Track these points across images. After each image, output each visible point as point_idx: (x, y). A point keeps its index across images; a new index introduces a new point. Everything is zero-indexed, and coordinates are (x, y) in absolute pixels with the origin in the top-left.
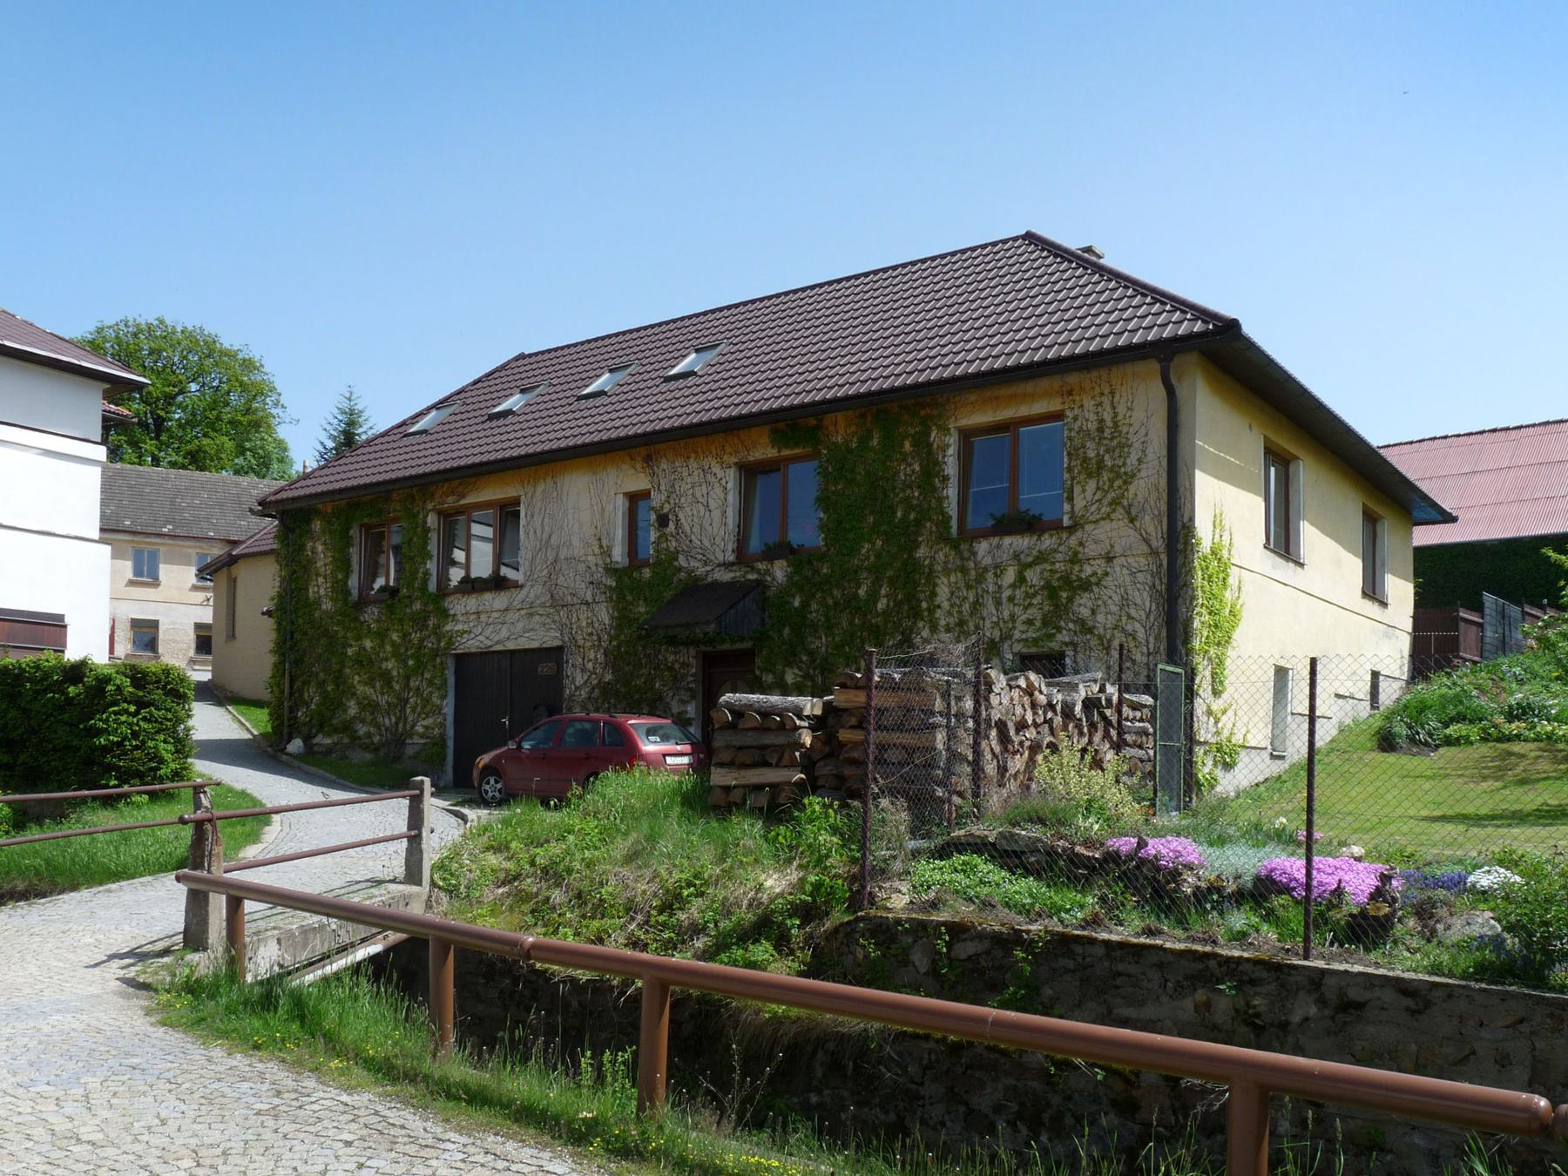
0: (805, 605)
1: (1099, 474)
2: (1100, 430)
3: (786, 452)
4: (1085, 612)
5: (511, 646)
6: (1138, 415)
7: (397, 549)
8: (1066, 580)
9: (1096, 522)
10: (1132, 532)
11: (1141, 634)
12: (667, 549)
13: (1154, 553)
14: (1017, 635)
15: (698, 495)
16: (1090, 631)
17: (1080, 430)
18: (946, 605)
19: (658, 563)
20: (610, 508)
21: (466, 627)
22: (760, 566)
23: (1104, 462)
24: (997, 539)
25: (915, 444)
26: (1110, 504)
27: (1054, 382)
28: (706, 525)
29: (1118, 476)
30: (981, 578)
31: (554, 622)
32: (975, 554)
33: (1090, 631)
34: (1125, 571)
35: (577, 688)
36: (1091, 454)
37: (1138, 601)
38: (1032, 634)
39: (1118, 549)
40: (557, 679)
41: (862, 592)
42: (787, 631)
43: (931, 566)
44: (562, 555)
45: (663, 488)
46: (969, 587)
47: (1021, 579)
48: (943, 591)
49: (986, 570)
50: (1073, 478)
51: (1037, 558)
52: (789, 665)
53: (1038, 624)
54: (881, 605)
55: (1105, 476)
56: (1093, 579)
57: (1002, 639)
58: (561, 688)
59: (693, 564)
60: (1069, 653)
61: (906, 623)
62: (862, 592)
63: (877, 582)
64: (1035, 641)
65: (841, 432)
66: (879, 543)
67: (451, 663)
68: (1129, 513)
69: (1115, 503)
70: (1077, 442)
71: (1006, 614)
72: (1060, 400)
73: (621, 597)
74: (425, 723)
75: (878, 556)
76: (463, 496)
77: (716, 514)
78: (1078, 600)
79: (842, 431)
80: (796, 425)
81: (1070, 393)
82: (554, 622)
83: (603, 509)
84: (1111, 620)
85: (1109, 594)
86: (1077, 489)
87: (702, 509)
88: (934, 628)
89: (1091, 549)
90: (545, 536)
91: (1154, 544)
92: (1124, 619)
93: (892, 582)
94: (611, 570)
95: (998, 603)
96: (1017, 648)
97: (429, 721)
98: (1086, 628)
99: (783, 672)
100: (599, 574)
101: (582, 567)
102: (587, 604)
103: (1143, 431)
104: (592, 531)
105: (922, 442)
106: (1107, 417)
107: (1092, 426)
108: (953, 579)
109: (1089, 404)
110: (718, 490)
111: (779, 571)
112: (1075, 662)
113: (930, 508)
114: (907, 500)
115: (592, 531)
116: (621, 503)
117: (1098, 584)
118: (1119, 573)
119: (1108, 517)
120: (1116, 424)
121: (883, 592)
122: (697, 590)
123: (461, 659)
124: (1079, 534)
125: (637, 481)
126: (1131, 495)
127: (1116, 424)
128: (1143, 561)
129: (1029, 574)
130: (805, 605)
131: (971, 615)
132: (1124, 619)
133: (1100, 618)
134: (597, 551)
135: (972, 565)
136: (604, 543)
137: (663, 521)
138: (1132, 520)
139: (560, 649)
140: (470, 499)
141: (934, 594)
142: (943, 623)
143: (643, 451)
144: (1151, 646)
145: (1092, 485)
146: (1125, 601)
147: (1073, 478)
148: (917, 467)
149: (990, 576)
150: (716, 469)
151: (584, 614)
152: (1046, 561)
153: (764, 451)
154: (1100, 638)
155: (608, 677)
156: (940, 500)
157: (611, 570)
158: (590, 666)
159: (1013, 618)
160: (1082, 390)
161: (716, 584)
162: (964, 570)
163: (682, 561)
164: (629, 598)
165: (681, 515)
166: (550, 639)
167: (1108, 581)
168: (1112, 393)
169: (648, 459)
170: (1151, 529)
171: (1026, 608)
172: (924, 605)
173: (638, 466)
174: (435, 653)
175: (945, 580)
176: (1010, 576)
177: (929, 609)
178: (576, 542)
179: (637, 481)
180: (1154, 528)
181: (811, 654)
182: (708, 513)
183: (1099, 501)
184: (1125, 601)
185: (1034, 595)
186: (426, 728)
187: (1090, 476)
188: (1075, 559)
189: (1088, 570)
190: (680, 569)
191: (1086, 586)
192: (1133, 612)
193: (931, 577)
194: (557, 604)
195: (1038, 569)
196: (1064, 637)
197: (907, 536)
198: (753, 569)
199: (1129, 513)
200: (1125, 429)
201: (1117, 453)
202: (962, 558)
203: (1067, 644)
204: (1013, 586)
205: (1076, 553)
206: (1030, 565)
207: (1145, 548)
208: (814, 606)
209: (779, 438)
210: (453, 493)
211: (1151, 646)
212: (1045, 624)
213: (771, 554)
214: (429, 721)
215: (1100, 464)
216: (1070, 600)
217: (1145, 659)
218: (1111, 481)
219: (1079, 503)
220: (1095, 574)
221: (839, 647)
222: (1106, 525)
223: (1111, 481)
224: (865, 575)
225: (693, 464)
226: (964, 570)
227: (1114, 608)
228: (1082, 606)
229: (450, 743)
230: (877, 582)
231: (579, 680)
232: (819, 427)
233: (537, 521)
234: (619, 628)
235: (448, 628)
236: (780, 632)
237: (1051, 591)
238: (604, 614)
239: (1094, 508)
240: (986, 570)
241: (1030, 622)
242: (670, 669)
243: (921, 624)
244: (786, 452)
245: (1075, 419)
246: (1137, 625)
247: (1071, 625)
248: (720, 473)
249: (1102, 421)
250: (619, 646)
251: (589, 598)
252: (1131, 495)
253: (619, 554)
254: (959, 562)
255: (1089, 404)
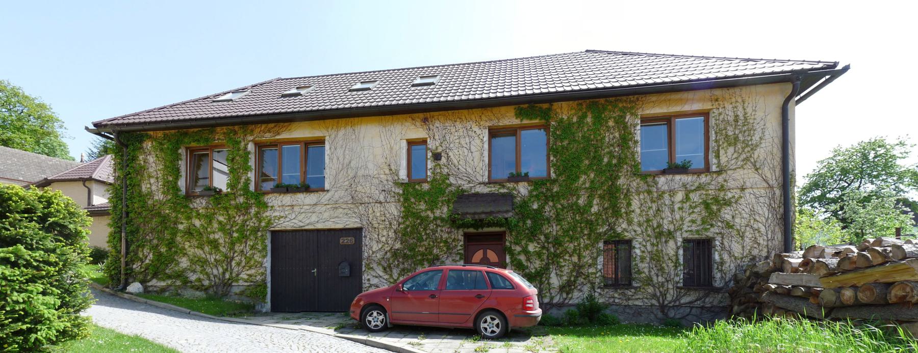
0: (542, 207)
1: (735, 144)
2: (736, 121)
3: (526, 122)
4: (728, 217)
5: (320, 226)
6: (760, 114)
7: (680, 265)
8: (716, 200)
9: (735, 169)
10: (757, 176)
11: (763, 229)
12: (441, 173)
13: (771, 187)
14: (685, 228)
15: (463, 142)
16: (732, 227)
17: (723, 120)
18: (638, 211)
19: (434, 180)
20: (396, 148)
21: (282, 214)
22: (508, 185)
23: (741, 136)
24: (671, 176)
25: (616, 122)
26: (743, 160)
27: (707, 93)
28: (469, 159)
29: (747, 145)
30: (660, 197)
31: (355, 213)
32: (656, 183)
33: (732, 227)
34: (752, 196)
35: (373, 253)
36: (730, 133)
37: (761, 212)
38: (694, 228)
39: (748, 185)
40: (358, 247)
41: (581, 202)
42: (529, 222)
43: (628, 190)
44: (360, 173)
45: (437, 137)
46: (652, 201)
47: (687, 198)
48: (635, 204)
49: (664, 192)
50: (719, 146)
51: (698, 187)
52: (530, 240)
53: (699, 222)
54: (595, 209)
55: (739, 146)
56: (733, 200)
57: (675, 231)
58: (360, 252)
59: (460, 182)
60: (719, 238)
61: (612, 220)
62: (581, 202)
63: (590, 198)
64: (697, 231)
65: (565, 112)
66: (592, 175)
67: (269, 236)
68: (755, 166)
69: (747, 159)
70: (722, 127)
71: (678, 217)
72: (710, 104)
73: (406, 200)
74: (249, 272)
75: (592, 182)
76: (279, 134)
77: (477, 155)
78: (723, 211)
79: (565, 112)
80: (535, 106)
81: (717, 100)
82: (355, 213)
83: (391, 148)
84: (744, 222)
85: (743, 208)
86: (722, 152)
87: (466, 151)
88: (630, 223)
89: (731, 184)
90: (346, 161)
91: (771, 183)
92: (752, 221)
93: (601, 197)
94: (397, 184)
95: (673, 211)
96: (685, 235)
97: (252, 272)
98: (729, 226)
99: (527, 245)
100: (390, 185)
101: (376, 181)
102: (381, 203)
103: (762, 123)
104: (383, 160)
105: (621, 123)
106: (740, 114)
107: (731, 119)
108: (642, 197)
109: (729, 107)
110: (478, 141)
111: (523, 189)
112: (722, 244)
113: (626, 157)
114: (610, 153)
115: (383, 160)
116: (404, 144)
117: (736, 202)
118: (748, 197)
119: (742, 167)
120: (746, 119)
121: (595, 202)
122: (462, 197)
123: (274, 233)
124: (724, 175)
125: (417, 132)
126: (756, 156)
127: (746, 119)
128: (763, 191)
129: (692, 195)
130: (542, 207)
131: (655, 216)
132: (752, 221)
133: (737, 220)
134: (387, 172)
135: (655, 190)
136: (393, 167)
137: (437, 157)
138: (757, 170)
139: (359, 230)
140: (284, 136)
141: (629, 204)
142: (636, 220)
143: (421, 115)
144: (769, 236)
145: (731, 150)
146: (753, 212)
147: (719, 146)
148: (617, 135)
149: (666, 196)
150: (476, 129)
151: (378, 209)
152: (703, 189)
153: (509, 119)
154: (738, 230)
155: (398, 246)
156: (633, 154)
157: (397, 184)
158: (384, 239)
159: (682, 219)
160: (724, 99)
161: (477, 195)
162: (649, 192)
163: (452, 180)
164: (413, 200)
165: (450, 154)
166: (352, 222)
167: (742, 201)
168: (743, 102)
169: (425, 120)
170: (769, 175)
171: (690, 214)
172: (623, 210)
173: (418, 124)
174: (256, 230)
175: (636, 197)
176: (680, 196)
177: (626, 213)
178: (370, 166)
179: (417, 132)
180: (773, 175)
181: (547, 236)
182: (468, 156)
183: (737, 158)
184: (753, 212)
185: (695, 207)
186: (250, 276)
187: (730, 145)
188: (722, 188)
189: (730, 195)
190: (451, 185)
191: (728, 203)
192: (757, 218)
193: (627, 195)
194: (356, 201)
195: (698, 193)
196: (715, 230)
197: (612, 173)
198: (504, 187)
199: (755, 166)
200: (751, 121)
201: (746, 134)
202: (648, 186)
203: (717, 234)
204: (682, 202)
205: (722, 186)
206: (693, 191)
207: (766, 185)
208: (547, 208)
209: (520, 114)
210: (269, 132)
211: (769, 236)
212: (703, 222)
213: (517, 178)
214: (252, 272)
215: (736, 139)
216: (719, 210)
217: (765, 243)
218: (743, 148)
219: (723, 159)
220: (734, 197)
221: (566, 232)
222: (741, 172)
223: (743, 148)
224: (582, 192)
225: (458, 125)
226: (649, 192)
227: (745, 215)
228: (727, 213)
229: (269, 285)
230: (590, 198)
231: (375, 248)
232: (550, 109)
233: (340, 152)
234: (406, 217)
235: (268, 214)
236: (524, 223)
237: (707, 206)
238: (394, 210)
239: (733, 162)
240: (664, 192)
241: (693, 221)
242: (446, 242)
243: (621, 221)
244: (526, 122)
245: (720, 114)
246: (760, 225)
247: (720, 224)
248: (478, 132)
249: (737, 116)
250: (406, 228)
251: (382, 198)
252: (756, 156)
253: (403, 175)
254: (646, 188)
255: (729, 107)
